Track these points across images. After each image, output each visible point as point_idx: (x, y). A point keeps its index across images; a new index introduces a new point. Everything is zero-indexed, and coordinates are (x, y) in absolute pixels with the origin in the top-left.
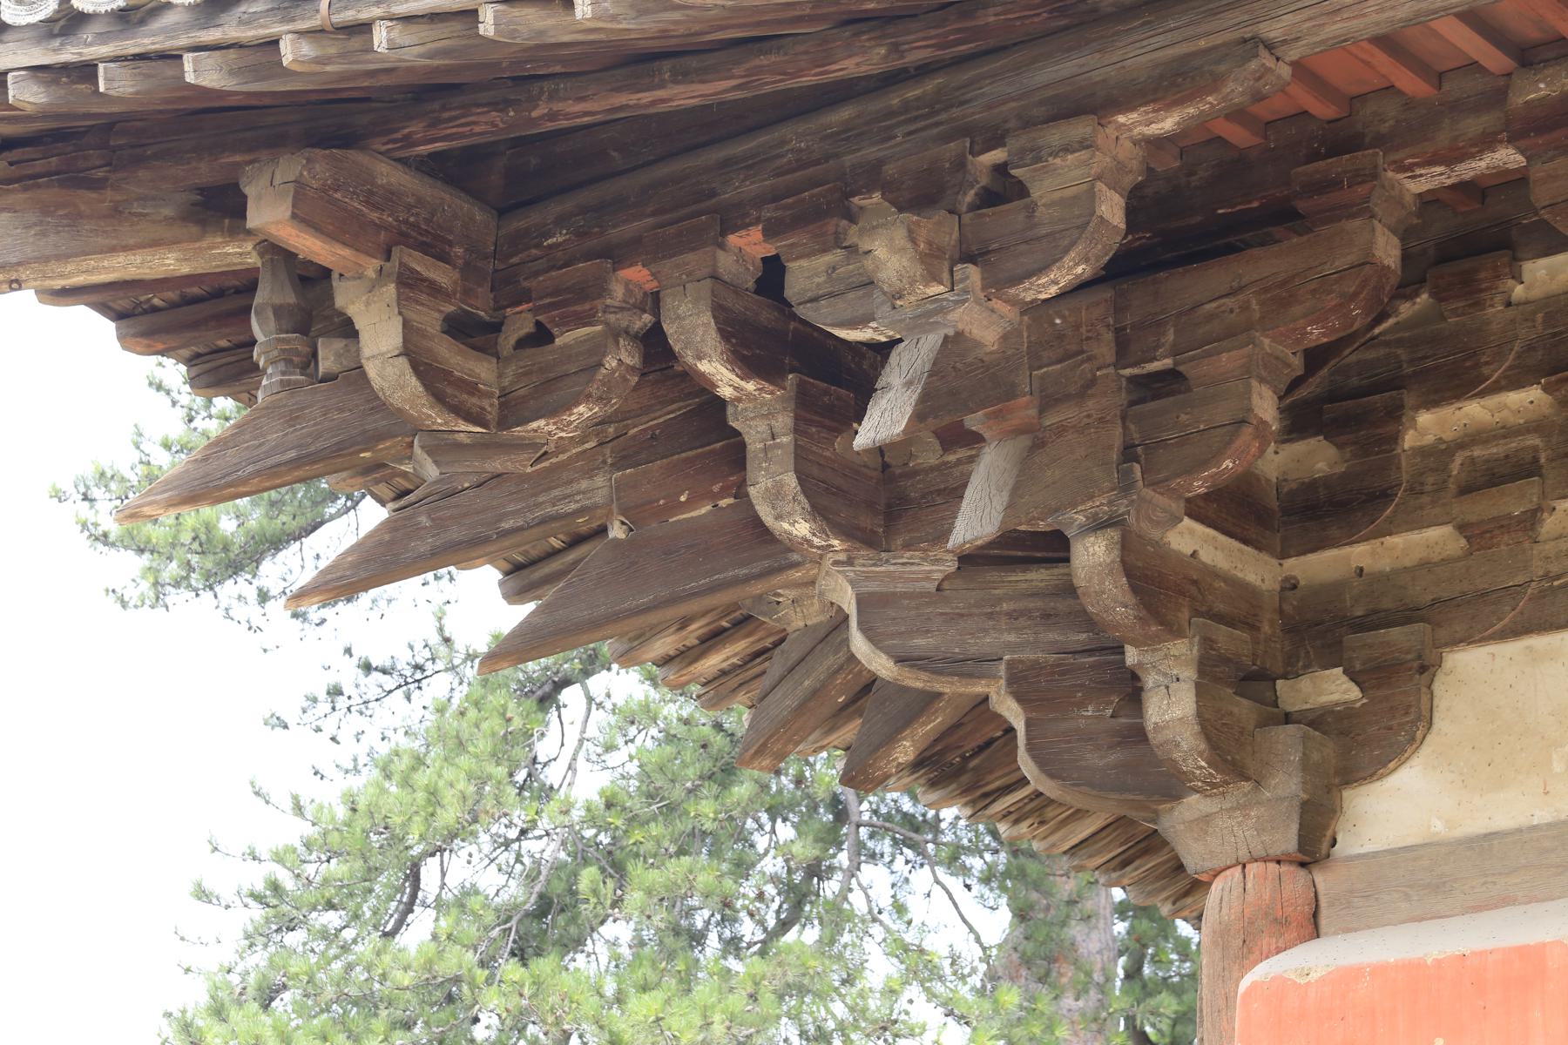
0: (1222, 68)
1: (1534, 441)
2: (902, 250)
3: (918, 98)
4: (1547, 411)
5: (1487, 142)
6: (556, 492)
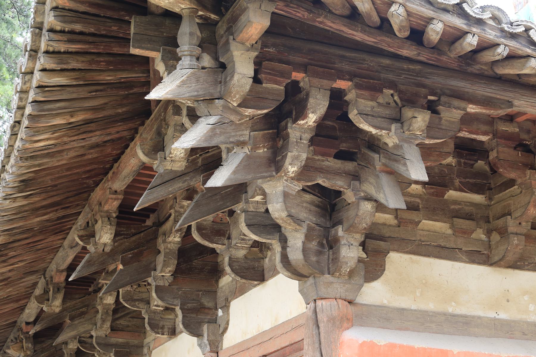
0: (503, 106)
1: (418, 200)
2: (425, 121)
3: (413, 69)
4: (421, 193)
5: (485, 133)
6: (240, 133)
